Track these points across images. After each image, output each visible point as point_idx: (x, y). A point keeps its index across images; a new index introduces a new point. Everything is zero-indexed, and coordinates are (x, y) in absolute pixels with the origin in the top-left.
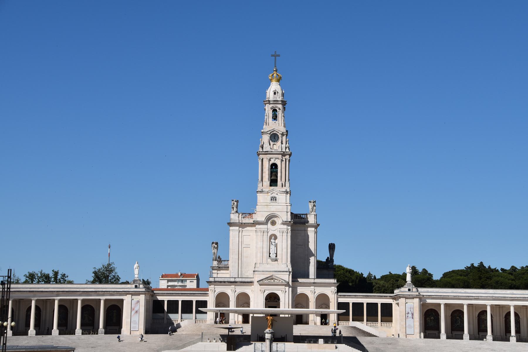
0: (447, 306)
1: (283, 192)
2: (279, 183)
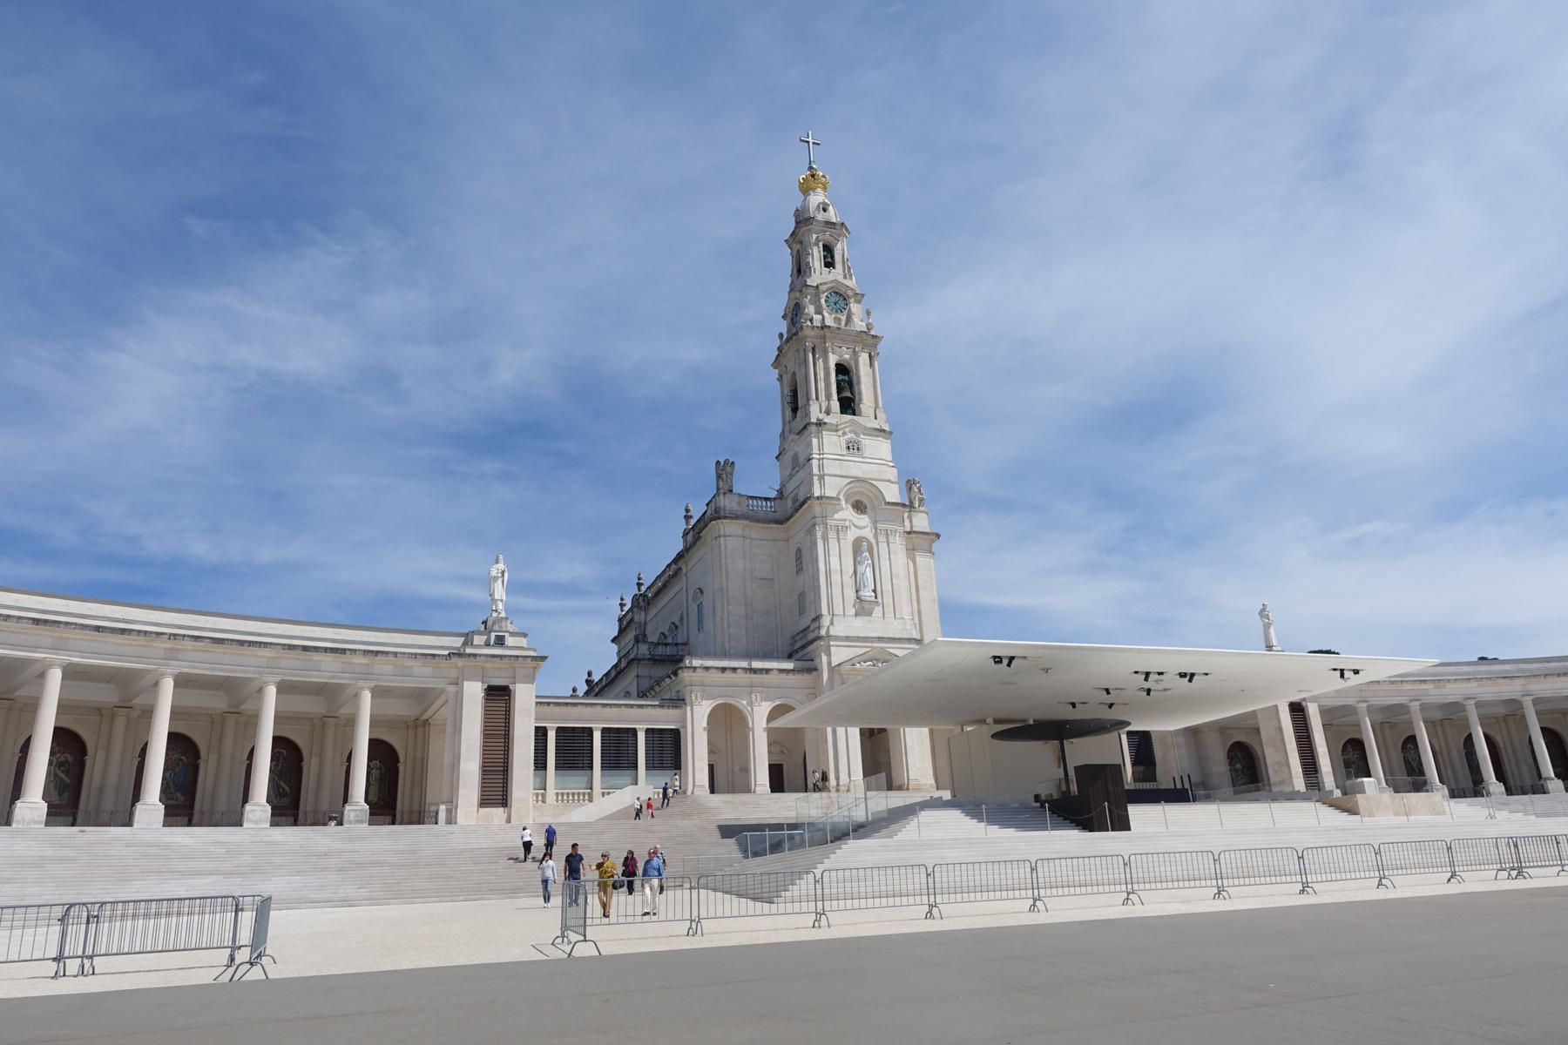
1: (875, 429)
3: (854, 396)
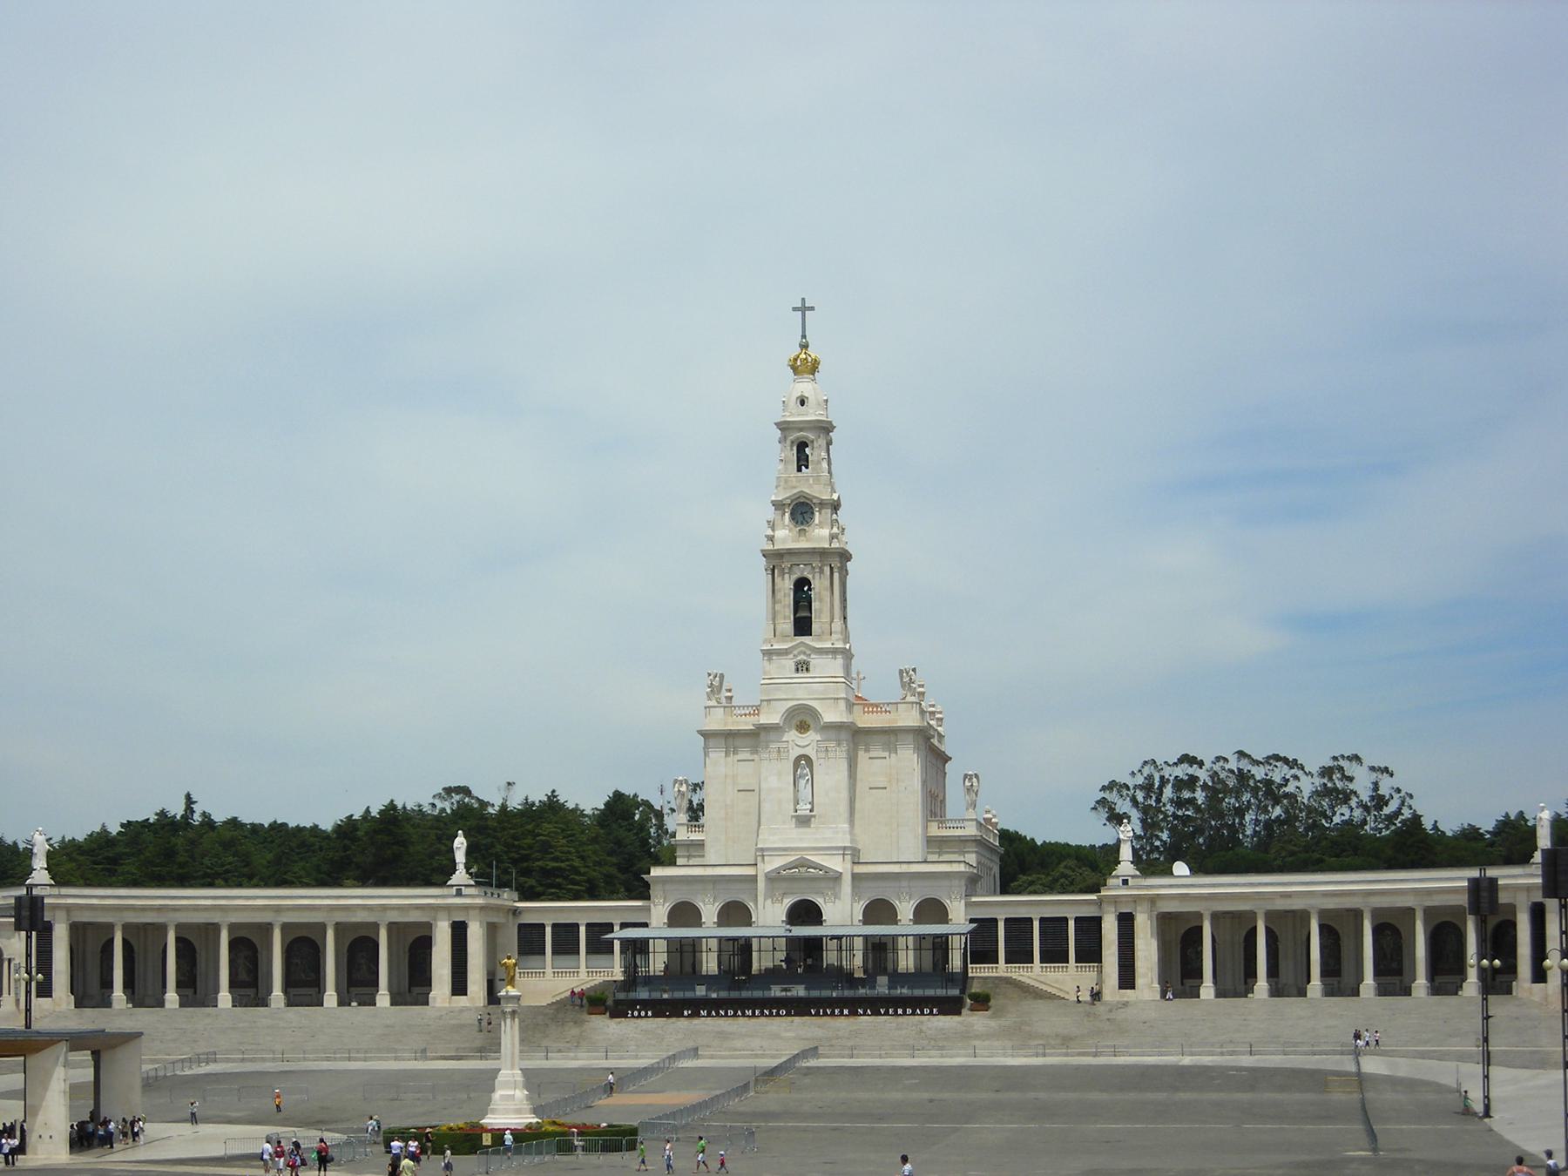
0: (1233, 918)
2: (814, 626)
3: (811, 613)
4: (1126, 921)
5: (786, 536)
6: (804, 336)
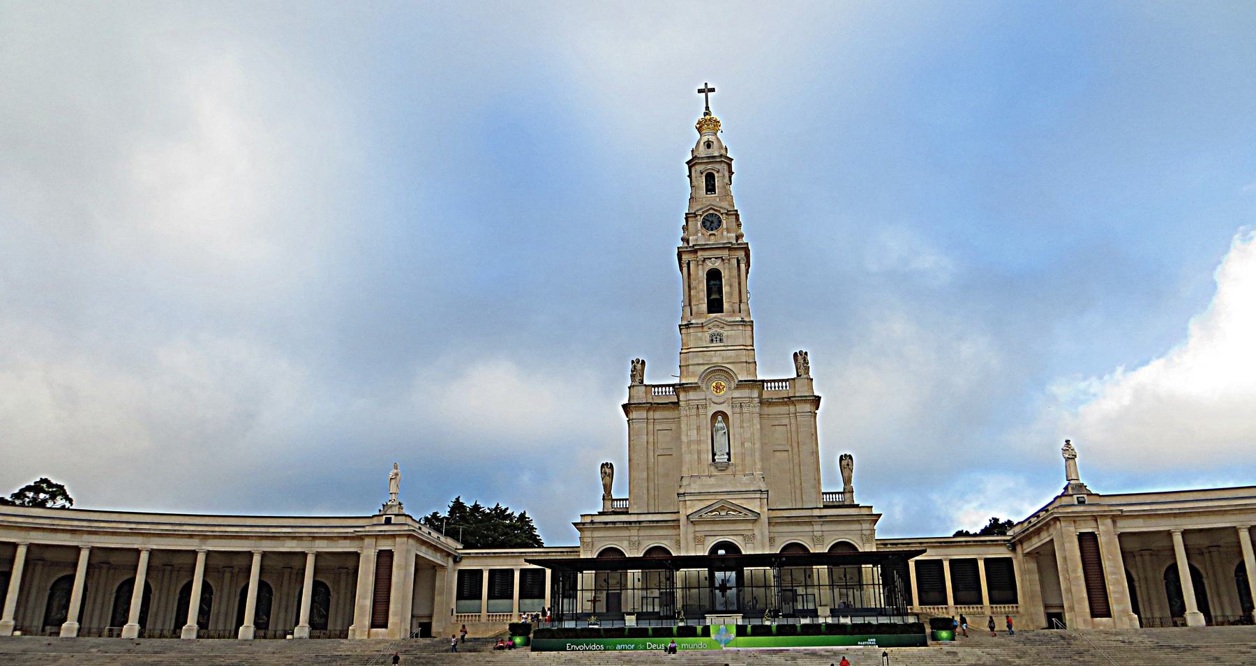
2: (726, 306)
4: (1088, 542)
5: (699, 237)
6: (707, 108)
